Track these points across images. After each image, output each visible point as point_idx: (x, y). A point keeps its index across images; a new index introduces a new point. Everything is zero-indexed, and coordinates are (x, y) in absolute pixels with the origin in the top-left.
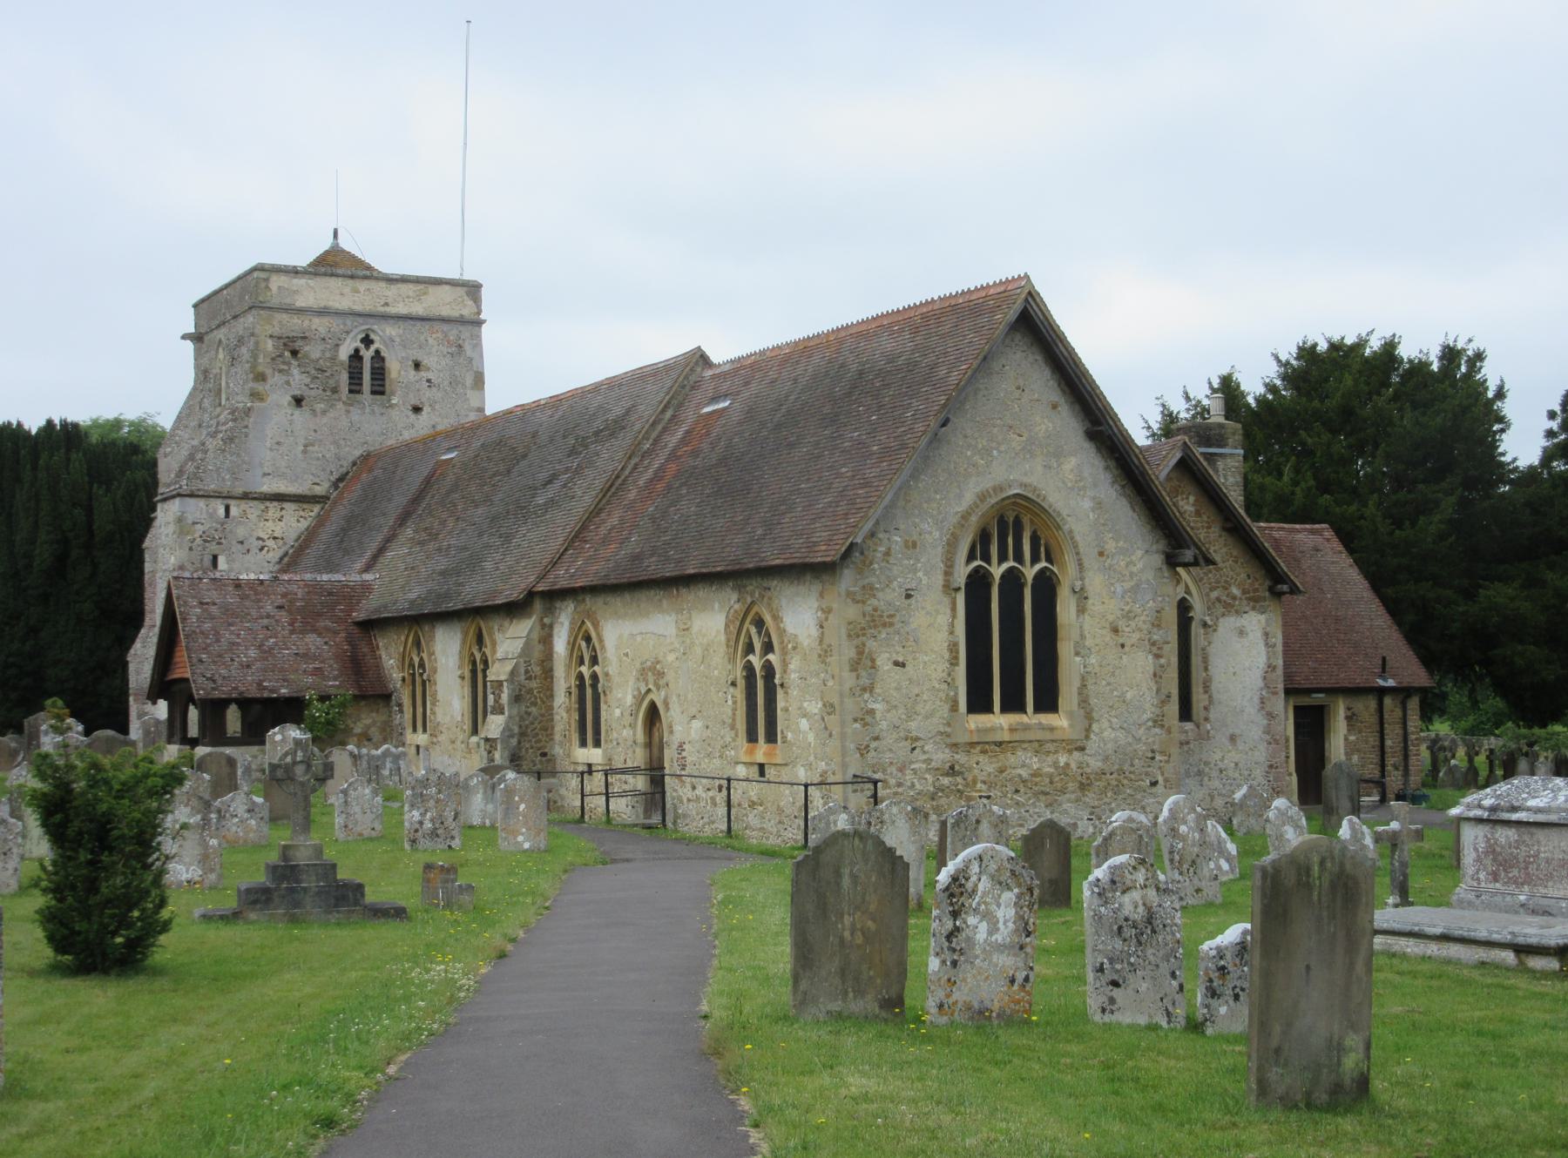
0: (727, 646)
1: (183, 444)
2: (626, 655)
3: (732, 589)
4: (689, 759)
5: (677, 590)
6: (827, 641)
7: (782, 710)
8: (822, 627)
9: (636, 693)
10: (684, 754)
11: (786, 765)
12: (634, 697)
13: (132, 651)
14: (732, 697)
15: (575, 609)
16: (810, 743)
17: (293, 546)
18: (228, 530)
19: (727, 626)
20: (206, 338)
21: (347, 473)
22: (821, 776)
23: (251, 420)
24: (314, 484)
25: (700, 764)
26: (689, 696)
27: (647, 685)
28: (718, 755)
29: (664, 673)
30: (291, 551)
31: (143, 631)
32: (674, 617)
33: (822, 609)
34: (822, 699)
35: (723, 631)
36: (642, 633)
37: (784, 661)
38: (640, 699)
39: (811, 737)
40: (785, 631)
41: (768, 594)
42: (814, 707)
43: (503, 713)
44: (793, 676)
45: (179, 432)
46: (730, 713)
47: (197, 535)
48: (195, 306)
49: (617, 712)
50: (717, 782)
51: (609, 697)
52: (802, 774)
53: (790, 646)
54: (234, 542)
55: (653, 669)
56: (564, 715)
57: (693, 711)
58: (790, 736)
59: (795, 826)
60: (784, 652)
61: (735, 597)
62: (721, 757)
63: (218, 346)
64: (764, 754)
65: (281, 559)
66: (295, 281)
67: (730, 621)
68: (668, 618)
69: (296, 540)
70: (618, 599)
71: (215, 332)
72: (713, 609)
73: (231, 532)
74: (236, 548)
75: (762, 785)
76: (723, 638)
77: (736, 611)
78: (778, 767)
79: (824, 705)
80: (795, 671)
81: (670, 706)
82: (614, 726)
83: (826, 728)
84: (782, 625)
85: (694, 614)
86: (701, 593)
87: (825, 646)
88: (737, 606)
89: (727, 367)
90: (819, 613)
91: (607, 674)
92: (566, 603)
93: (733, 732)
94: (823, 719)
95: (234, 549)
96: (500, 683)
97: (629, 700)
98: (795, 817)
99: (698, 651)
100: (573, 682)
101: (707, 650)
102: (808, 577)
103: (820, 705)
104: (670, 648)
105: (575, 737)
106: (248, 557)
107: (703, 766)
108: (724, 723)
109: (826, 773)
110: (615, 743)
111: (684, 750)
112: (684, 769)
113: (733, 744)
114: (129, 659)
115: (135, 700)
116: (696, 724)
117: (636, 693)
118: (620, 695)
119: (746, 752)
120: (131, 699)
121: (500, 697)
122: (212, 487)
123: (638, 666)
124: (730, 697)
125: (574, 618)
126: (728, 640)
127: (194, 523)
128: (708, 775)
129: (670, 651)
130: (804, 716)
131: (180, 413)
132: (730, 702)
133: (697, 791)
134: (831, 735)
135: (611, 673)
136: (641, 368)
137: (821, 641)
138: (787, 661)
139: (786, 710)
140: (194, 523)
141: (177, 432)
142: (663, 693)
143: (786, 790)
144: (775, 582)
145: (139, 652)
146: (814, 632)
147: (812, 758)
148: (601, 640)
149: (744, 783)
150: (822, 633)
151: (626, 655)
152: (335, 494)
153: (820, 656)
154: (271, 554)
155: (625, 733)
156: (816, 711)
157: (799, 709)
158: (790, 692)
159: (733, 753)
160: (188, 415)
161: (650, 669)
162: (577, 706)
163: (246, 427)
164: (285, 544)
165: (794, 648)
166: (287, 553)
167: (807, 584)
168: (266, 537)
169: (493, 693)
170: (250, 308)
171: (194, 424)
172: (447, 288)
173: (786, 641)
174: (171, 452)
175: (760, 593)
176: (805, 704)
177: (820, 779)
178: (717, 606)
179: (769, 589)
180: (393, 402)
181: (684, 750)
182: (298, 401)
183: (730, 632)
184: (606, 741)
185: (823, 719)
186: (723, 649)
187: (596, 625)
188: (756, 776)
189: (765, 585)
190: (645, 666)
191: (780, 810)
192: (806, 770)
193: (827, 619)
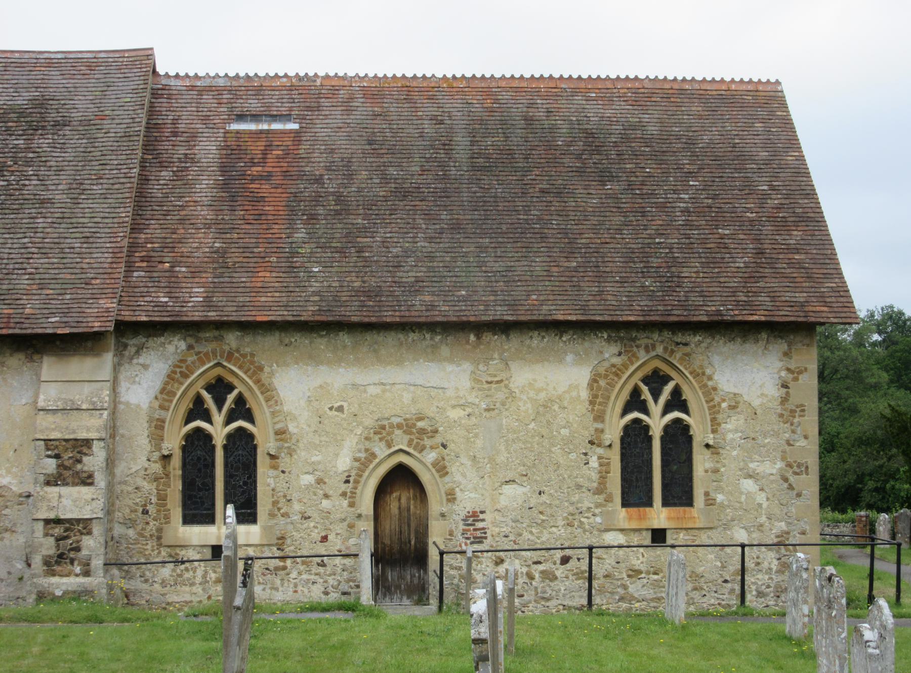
0: (592, 403)
2: (340, 409)
3: (609, 340)
4: (492, 530)
5: (478, 337)
6: (794, 400)
7: (706, 471)
8: (785, 386)
9: (362, 455)
10: (480, 525)
11: (711, 528)
12: (356, 460)
14: (600, 458)
15: (190, 347)
16: (760, 505)
19: (594, 381)
22: (777, 537)
25: (520, 535)
26: (501, 458)
27: (389, 446)
28: (561, 523)
29: (436, 431)
32: (467, 366)
33: (788, 370)
34: (783, 459)
35: (586, 385)
36: (383, 384)
37: (713, 420)
38: (365, 462)
39: (761, 498)
40: (715, 389)
41: (687, 349)
42: (772, 467)
43: (91, 484)
44: (730, 436)
46: (595, 476)
49: (308, 479)
50: (558, 555)
51: (284, 462)
52: (742, 536)
53: (724, 405)
55: (408, 427)
56: (146, 486)
57: (510, 475)
58: (720, 498)
59: (726, 591)
60: (714, 410)
61: (614, 349)
62: (570, 525)
64: (669, 518)
67: (599, 375)
68: (450, 368)
70: (324, 341)
72: (561, 361)
75: (659, 551)
76: (584, 394)
77: (613, 366)
78: (696, 532)
79: (789, 465)
80: (736, 431)
81: (453, 469)
82: (295, 496)
83: (791, 487)
84: (710, 383)
85: (514, 366)
86: (535, 342)
87: (790, 406)
88: (617, 360)
89: (221, 82)
90: (783, 374)
91: (281, 434)
92: (162, 339)
93: (600, 499)
94: (786, 480)
96: (87, 443)
97: (344, 463)
98: (726, 581)
99: (526, 407)
100: (173, 443)
101: (545, 406)
102: (764, 335)
103: (779, 465)
104: (453, 402)
105: (177, 513)
107: (526, 535)
108: (579, 487)
109: (788, 533)
110: (296, 518)
111: (483, 520)
112: (481, 542)
113: (597, 511)
116: (508, 489)
117: (362, 455)
118: (314, 459)
119: (630, 519)
121: (79, 461)
123: (369, 422)
124: (595, 458)
125: (181, 361)
126: (595, 396)
128: (539, 546)
129: (454, 407)
130: (750, 477)
132: (594, 463)
133: (505, 565)
134: (799, 495)
135: (292, 428)
136: (12, 52)
137: (784, 400)
138: (720, 417)
139: (716, 471)
142: (431, 456)
143: (710, 555)
144: (698, 338)
146: (773, 391)
147: (763, 519)
148: (268, 391)
149: (621, 552)
150: (787, 394)
151: (340, 409)
153: (781, 415)
155: (325, 503)
156: (774, 471)
157: (741, 470)
158: (721, 451)
159: (598, 519)
161: (399, 426)
162: (180, 472)
165: (732, 408)
167: (762, 343)
169: (57, 456)
173: (717, 399)
175: (665, 349)
176: (752, 465)
177: (776, 540)
178: (569, 358)
179: (686, 344)
181: (483, 520)
183: (599, 388)
184: (272, 515)
185: (786, 480)
186: (583, 407)
187: (256, 371)
188: (648, 541)
189: (679, 340)
190: (386, 423)
191: (695, 576)
192: (749, 533)
193: (796, 379)
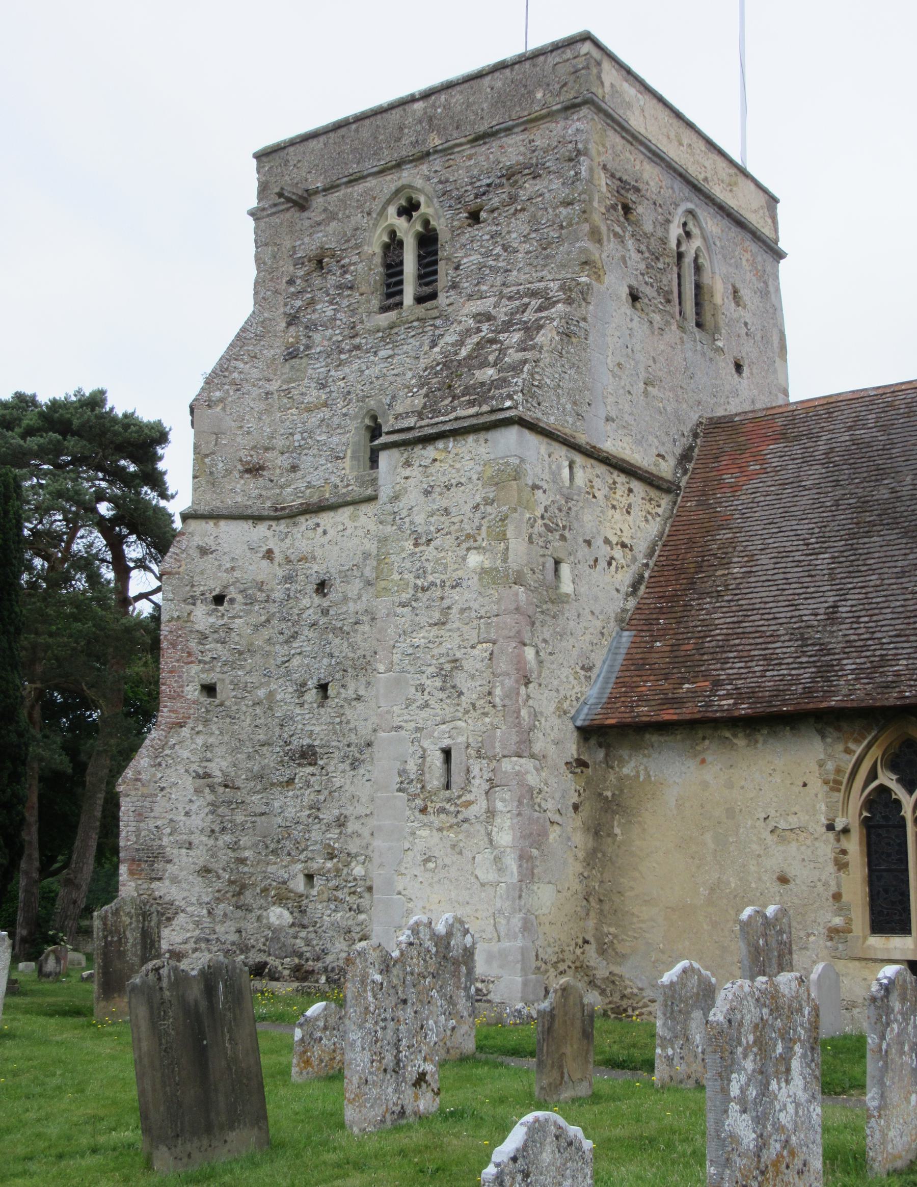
1: (247, 387)
13: (129, 773)
17: (647, 565)
18: (573, 513)
20: (319, 201)
21: (691, 448)
23: (591, 307)
24: (659, 455)
30: (646, 575)
31: (154, 734)
45: (240, 365)
47: (539, 512)
48: (262, 156)
54: (581, 540)
63: (389, 202)
65: (635, 586)
66: (626, 85)
69: (650, 555)
71: (371, 182)
73: (577, 518)
74: (583, 552)
95: (580, 555)
106: (596, 574)
114: (120, 788)
115: (131, 873)
120: (123, 869)
122: (552, 419)
127: (535, 487)
131: (244, 330)
140: (535, 487)
141: (234, 363)
145: (143, 777)
152: (685, 479)
154: (619, 576)
160: (259, 337)
163: (585, 320)
164: (634, 559)
166: (642, 577)
168: (614, 540)
170: (571, 107)
171: (277, 350)
172: (752, 186)
174: (221, 400)
180: (720, 344)
182: (634, 297)
